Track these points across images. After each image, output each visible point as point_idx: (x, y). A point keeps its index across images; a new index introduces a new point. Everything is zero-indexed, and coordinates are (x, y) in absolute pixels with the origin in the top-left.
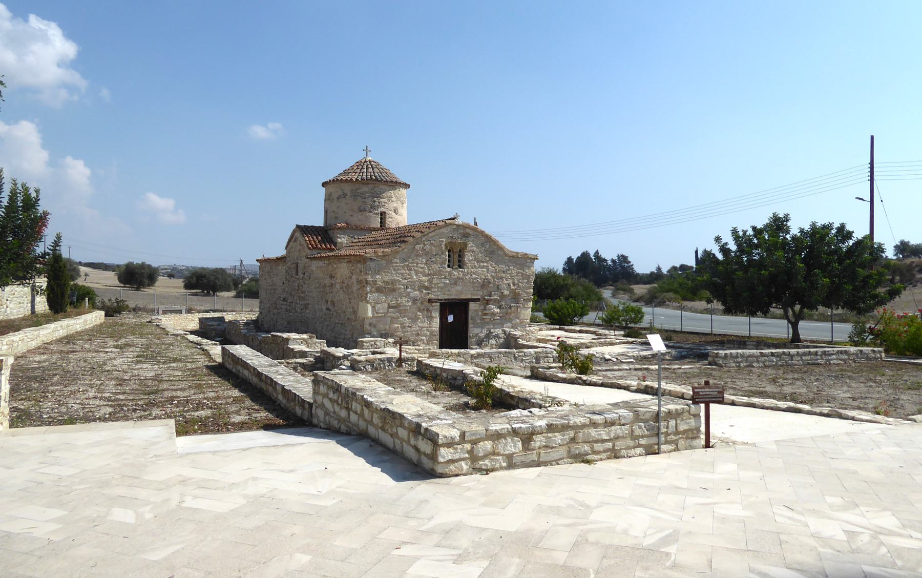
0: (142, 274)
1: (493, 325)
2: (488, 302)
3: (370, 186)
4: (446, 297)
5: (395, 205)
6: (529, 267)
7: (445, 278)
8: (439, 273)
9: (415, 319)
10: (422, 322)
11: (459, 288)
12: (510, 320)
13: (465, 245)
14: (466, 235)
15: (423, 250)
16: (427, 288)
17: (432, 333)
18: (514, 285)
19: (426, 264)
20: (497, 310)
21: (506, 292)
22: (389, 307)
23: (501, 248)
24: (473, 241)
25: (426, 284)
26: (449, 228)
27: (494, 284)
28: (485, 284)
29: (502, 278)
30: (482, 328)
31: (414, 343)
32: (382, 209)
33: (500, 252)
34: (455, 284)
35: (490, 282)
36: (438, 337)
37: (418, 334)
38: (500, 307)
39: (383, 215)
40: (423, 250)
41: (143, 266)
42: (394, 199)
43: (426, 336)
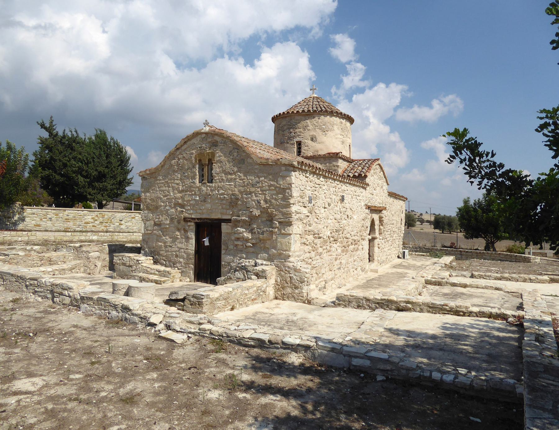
1: (247, 253)
2: (237, 223)
3: (287, 119)
4: (199, 216)
5: (312, 133)
6: (284, 177)
7: (195, 194)
8: (189, 189)
9: (175, 239)
10: (181, 243)
11: (209, 206)
12: (266, 250)
13: (213, 154)
14: (215, 144)
15: (178, 165)
16: (182, 206)
17: (188, 255)
18: (266, 201)
19: (181, 179)
20: (250, 236)
21: (257, 212)
22: (155, 224)
23: (248, 156)
24: (221, 150)
25: (180, 201)
26: (199, 138)
27: (243, 202)
28: (233, 202)
29: (251, 193)
30: (235, 256)
31: (174, 264)
32: (298, 139)
33: (249, 160)
34: (205, 201)
36: (193, 261)
37: (177, 256)
38: (252, 231)
41: (444, 217)
42: (311, 127)
43: (184, 258)
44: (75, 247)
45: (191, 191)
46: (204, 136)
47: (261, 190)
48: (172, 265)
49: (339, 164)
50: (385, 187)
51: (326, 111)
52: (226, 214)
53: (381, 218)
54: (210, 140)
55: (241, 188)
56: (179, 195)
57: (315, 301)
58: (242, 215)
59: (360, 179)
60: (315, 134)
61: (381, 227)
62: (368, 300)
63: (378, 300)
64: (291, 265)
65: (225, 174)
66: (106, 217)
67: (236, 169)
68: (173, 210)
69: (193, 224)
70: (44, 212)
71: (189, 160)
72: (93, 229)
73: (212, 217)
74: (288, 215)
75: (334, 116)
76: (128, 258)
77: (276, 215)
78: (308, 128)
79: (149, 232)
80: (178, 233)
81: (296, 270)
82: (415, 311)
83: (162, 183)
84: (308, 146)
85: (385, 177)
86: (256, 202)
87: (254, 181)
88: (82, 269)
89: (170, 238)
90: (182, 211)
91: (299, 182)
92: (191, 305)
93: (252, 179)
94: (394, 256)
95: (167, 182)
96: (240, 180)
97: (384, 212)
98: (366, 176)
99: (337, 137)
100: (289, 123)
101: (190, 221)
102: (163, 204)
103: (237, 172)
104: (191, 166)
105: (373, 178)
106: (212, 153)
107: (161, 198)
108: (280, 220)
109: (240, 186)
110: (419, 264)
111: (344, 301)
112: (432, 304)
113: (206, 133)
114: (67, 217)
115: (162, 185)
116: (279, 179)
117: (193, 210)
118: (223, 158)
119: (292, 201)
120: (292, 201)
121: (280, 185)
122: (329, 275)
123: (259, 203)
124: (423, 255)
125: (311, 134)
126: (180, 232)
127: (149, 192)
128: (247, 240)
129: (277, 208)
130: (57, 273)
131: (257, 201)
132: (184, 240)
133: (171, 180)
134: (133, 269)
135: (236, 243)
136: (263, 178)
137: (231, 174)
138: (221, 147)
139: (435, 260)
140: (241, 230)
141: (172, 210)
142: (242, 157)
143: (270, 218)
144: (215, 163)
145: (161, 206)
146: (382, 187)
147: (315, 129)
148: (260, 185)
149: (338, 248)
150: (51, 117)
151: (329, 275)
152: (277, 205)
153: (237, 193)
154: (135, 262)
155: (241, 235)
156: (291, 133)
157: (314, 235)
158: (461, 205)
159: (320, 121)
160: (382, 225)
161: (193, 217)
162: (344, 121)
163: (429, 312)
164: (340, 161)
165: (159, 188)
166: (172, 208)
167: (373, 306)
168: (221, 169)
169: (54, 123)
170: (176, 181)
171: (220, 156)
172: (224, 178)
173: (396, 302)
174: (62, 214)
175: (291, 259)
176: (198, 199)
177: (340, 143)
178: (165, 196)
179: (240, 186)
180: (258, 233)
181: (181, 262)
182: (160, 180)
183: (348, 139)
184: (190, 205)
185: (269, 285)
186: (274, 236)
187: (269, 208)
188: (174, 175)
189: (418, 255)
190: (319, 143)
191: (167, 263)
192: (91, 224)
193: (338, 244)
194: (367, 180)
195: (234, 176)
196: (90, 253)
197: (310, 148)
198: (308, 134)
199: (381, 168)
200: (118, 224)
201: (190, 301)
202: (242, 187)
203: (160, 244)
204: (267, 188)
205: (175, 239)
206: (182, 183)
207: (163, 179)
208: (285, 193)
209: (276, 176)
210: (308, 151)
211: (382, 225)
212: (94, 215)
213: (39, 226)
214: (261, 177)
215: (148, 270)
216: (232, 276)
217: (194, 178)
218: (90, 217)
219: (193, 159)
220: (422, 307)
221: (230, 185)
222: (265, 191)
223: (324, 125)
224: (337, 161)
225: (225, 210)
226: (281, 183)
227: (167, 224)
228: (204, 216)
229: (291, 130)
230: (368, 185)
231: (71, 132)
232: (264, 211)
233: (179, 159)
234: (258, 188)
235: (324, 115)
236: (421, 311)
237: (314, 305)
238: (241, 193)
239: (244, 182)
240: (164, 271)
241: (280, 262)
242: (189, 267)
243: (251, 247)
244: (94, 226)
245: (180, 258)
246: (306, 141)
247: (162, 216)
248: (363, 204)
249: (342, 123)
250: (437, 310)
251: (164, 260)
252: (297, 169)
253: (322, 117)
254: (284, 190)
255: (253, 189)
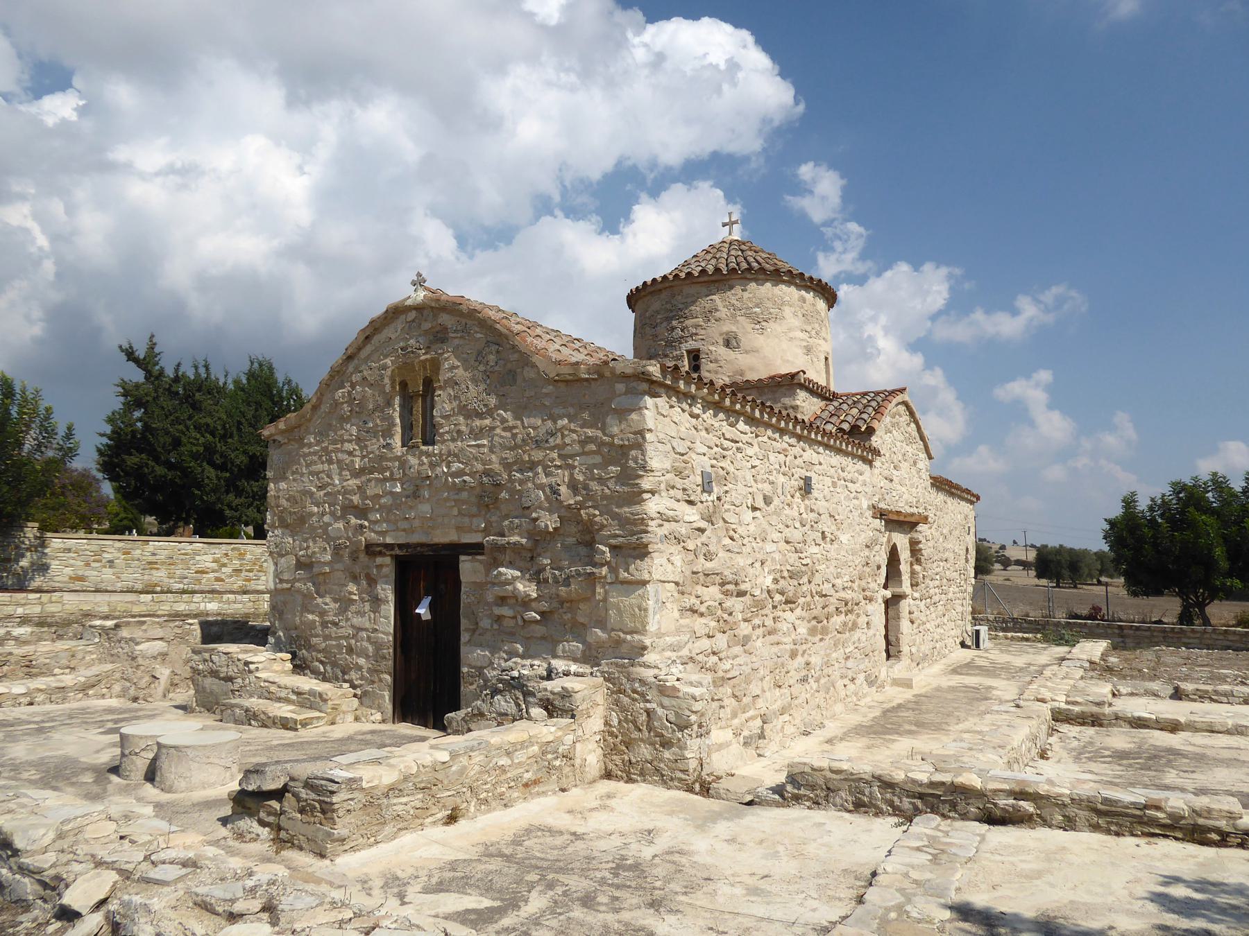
0: (1059, 562)
1: (526, 641)
2: (497, 555)
3: (664, 295)
6: (622, 413)
7: (392, 479)
8: (377, 465)
9: (345, 604)
11: (425, 508)
12: (578, 630)
13: (436, 365)
14: (439, 337)
16: (362, 512)
17: (378, 646)
18: (574, 486)
19: (359, 440)
21: (549, 521)
22: (300, 565)
23: (525, 359)
25: (356, 499)
26: (399, 324)
27: (513, 492)
28: (488, 496)
29: (532, 466)
30: (494, 649)
31: (344, 673)
32: (691, 344)
33: (529, 373)
35: (498, 485)
36: (391, 663)
37: (350, 650)
38: (537, 577)
39: (695, 356)
40: (351, 400)
41: (1060, 550)
42: (723, 312)
43: (367, 657)
44: (103, 628)
45: (382, 470)
46: (412, 315)
47: (560, 456)
48: (340, 675)
49: (798, 403)
50: (924, 463)
51: (762, 270)
52: (470, 530)
53: (914, 544)
54: (426, 326)
55: (508, 454)
56: (353, 483)
57: (724, 784)
58: (511, 529)
59: (856, 438)
60: (734, 329)
61: (917, 568)
62: (887, 785)
63: (921, 785)
64: (648, 674)
65: (468, 416)
66: (248, 556)
67: (493, 401)
68: (340, 525)
69: (388, 560)
70: (94, 545)
71: (376, 385)
72: (217, 586)
73: (436, 540)
74: (637, 525)
75: (784, 282)
76: (224, 658)
77: (603, 527)
78: (717, 314)
79: (285, 586)
80: (352, 587)
81: (663, 690)
82: (1046, 823)
83: (315, 453)
84: (716, 361)
85: (922, 438)
86: (547, 490)
87: (542, 431)
88: (117, 688)
89: (335, 600)
90: (361, 526)
91: (666, 425)
92: (302, 811)
93: (536, 424)
94: (953, 643)
95: (325, 449)
96: (504, 429)
97: (921, 527)
98: (871, 431)
99: (791, 335)
100: (669, 306)
101: (380, 554)
102: (315, 509)
103: (497, 408)
104: (381, 401)
105: (890, 435)
106: (432, 360)
107: (312, 494)
108: (613, 541)
109: (503, 447)
110: (1019, 661)
111: (812, 787)
112: (1106, 801)
113: (419, 308)
115: (315, 458)
116: (609, 420)
117: (387, 521)
118: (460, 372)
119: (646, 484)
120: (646, 484)
121: (612, 437)
122: (772, 700)
123: (556, 492)
124: (1027, 640)
125: (725, 329)
126: (358, 584)
127: (284, 478)
128: (526, 603)
129: (608, 503)
130: (40, 697)
131: (551, 487)
132: (367, 606)
133: (335, 442)
134: (236, 687)
135: (498, 611)
136: (566, 421)
137: (480, 416)
138: (456, 342)
139: (1061, 650)
140: (509, 573)
141: (336, 525)
142: (509, 366)
143: (588, 538)
144: (440, 388)
145: (311, 514)
146: (915, 463)
147: (734, 316)
148: (559, 441)
149: (797, 622)
150: (152, 336)
151: (772, 700)
152: (604, 497)
153: (496, 466)
154: (241, 666)
155: (509, 588)
156: (673, 329)
157: (722, 584)
158: (1117, 511)
159: (746, 295)
160: (918, 561)
161: (389, 540)
162: (809, 296)
163: (1095, 828)
164: (802, 394)
165: (308, 466)
166: (337, 519)
167: (906, 804)
168: (455, 404)
169: (157, 350)
170: (349, 447)
171: (453, 367)
172: (463, 428)
173: (980, 794)
174: (139, 552)
175: (650, 657)
176: (398, 490)
177: (800, 351)
178: (320, 488)
179: (503, 447)
180: (556, 581)
181: (360, 668)
182: (310, 445)
183: (821, 342)
184: (382, 508)
185: (586, 740)
186: (599, 590)
187: (581, 505)
188: (342, 428)
189: (1013, 638)
190: (747, 352)
191: (329, 668)
192: (211, 575)
193: (798, 612)
194: (875, 441)
195: (487, 422)
196: (137, 644)
197: (724, 366)
198: (715, 331)
199: (912, 414)
201: (296, 795)
202: (511, 449)
203: (310, 617)
204: (577, 447)
205: (345, 604)
206: (361, 449)
207: (318, 443)
208: (625, 459)
209: (599, 413)
210: (716, 372)
211: (918, 561)
213: (81, 579)
214: (561, 418)
215: (273, 688)
216: (485, 708)
217: (388, 433)
218: (209, 558)
219: (387, 381)
220: (1072, 811)
221: (478, 446)
222: (572, 456)
223: (757, 306)
224: (793, 395)
225: (466, 520)
226: (615, 430)
227: (325, 564)
228: (415, 538)
229: (674, 323)
230: (877, 452)
231: (196, 367)
232: (570, 516)
233: (353, 386)
234: (552, 449)
235: (756, 280)
236: (1069, 824)
237: (719, 797)
238: (507, 466)
239: (514, 436)
240: (312, 693)
241: (617, 665)
242: (381, 680)
243: (537, 622)
244: (218, 579)
245: (359, 656)
246: (711, 348)
247: (315, 542)
248: (865, 504)
249: (804, 300)
250: (1126, 822)
251: (322, 662)
252: (662, 390)
253: (753, 285)
254: (624, 450)
255: (538, 455)
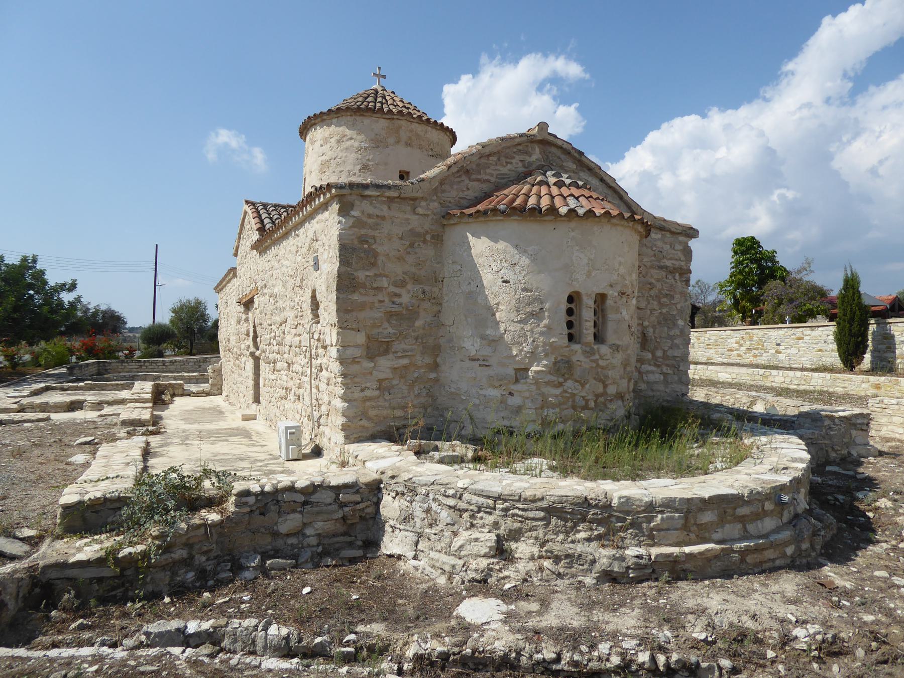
66: (755, 339)
114: (708, 342)
192: (736, 352)
200: (773, 351)
212: (738, 335)
218: (733, 340)
244: (739, 356)
